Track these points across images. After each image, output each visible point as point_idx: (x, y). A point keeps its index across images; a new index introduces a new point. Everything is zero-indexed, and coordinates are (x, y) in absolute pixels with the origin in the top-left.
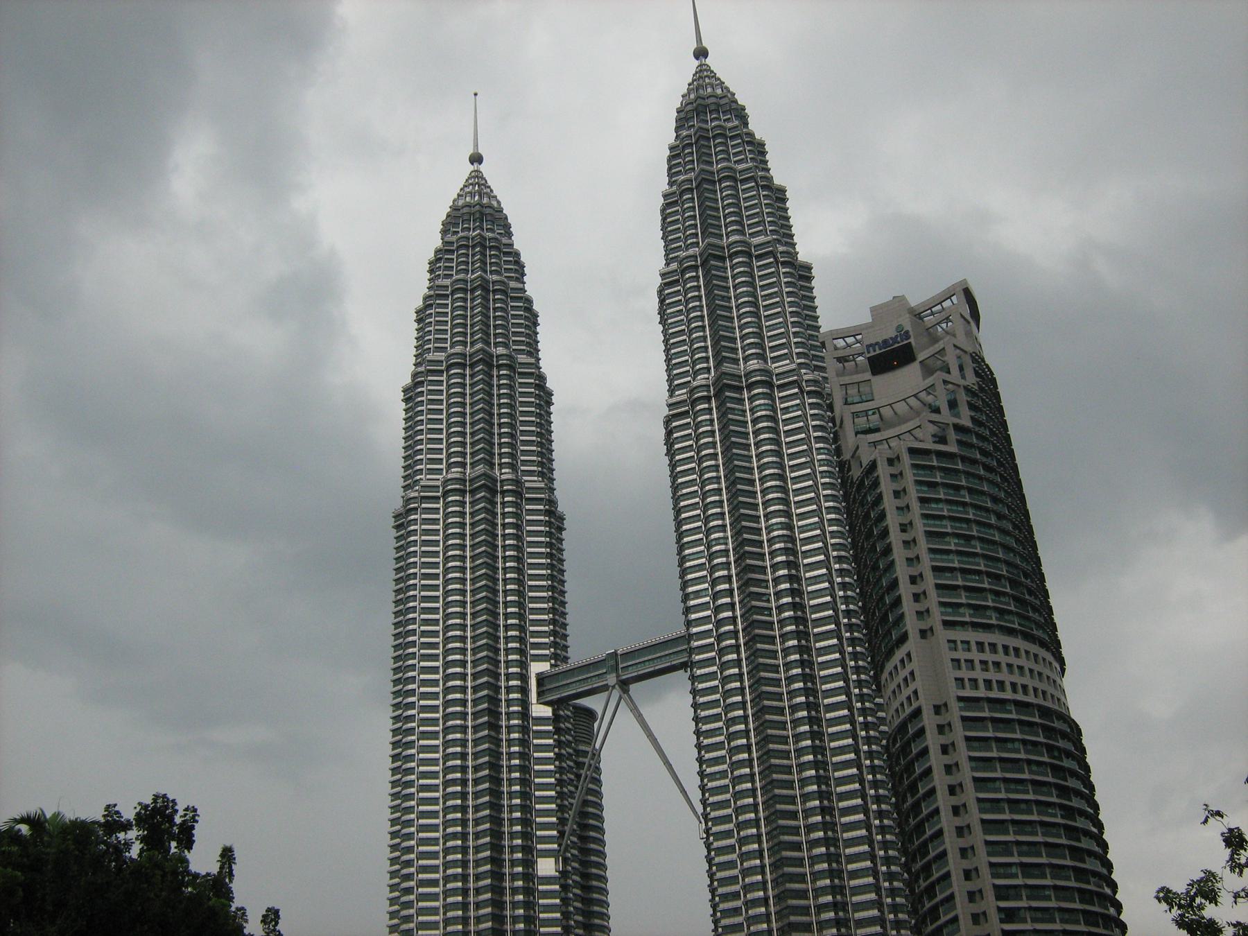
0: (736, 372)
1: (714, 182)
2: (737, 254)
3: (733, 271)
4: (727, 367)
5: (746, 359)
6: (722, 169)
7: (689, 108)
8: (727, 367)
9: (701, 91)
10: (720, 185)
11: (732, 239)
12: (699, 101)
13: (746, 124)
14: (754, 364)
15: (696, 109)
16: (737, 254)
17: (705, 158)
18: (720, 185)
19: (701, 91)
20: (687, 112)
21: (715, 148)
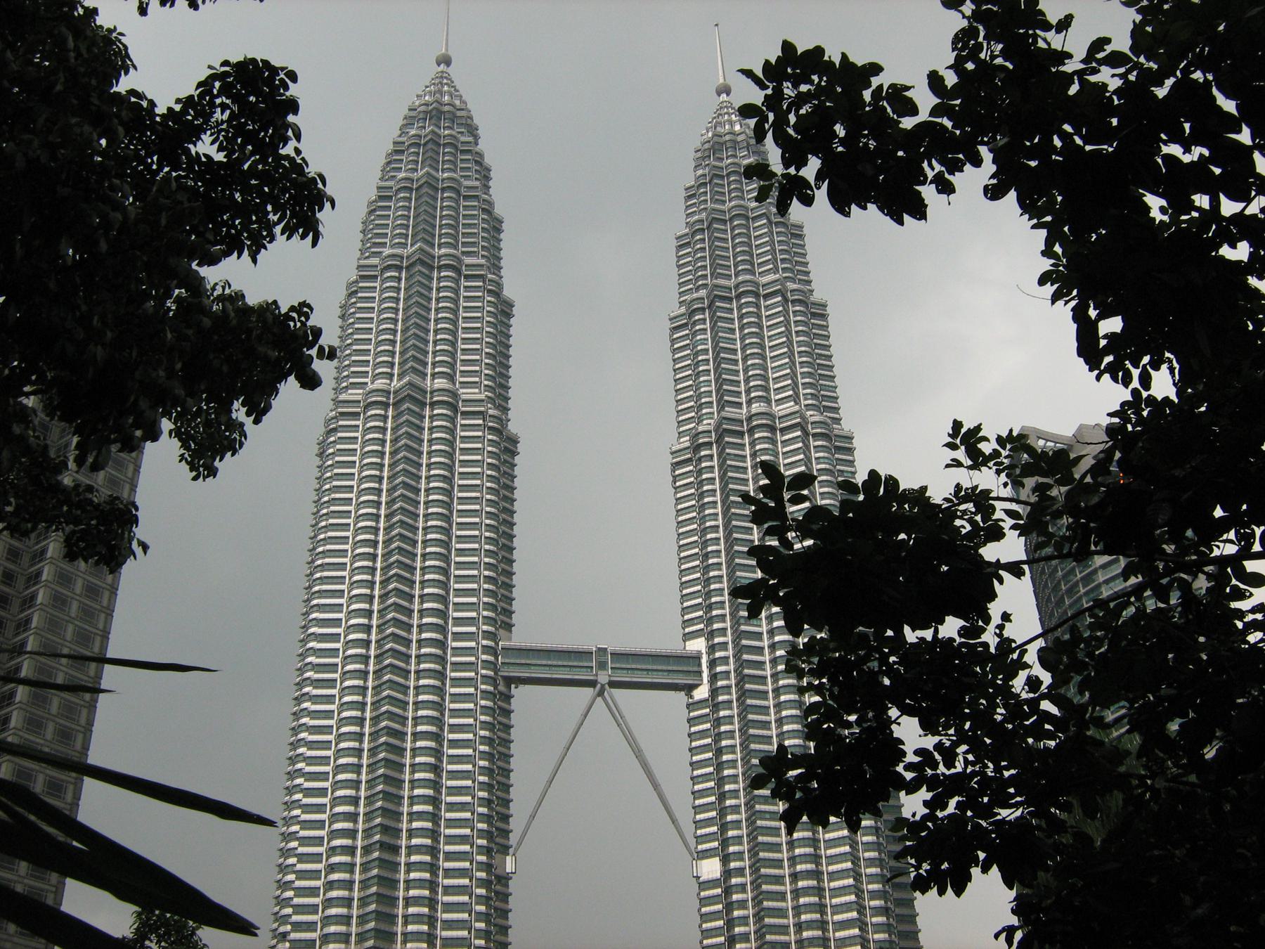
0: (737, 416)
1: (437, 189)
2: (447, 267)
3: (440, 282)
4: (730, 412)
5: (434, 376)
6: (448, 178)
7: (707, 146)
8: (730, 412)
9: (719, 129)
10: (442, 194)
11: (443, 251)
12: (716, 139)
13: (477, 144)
14: (440, 383)
15: (713, 146)
16: (447, 267)
17: (718, 198)
18: (442, 194)
19: (719, 129)
20: (420, 112)
21: (445, 154)
